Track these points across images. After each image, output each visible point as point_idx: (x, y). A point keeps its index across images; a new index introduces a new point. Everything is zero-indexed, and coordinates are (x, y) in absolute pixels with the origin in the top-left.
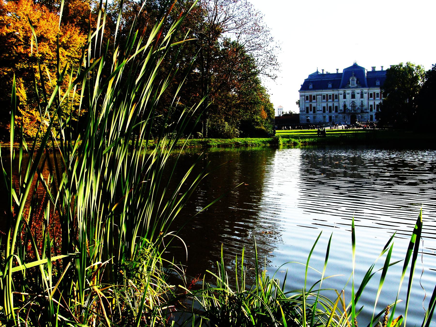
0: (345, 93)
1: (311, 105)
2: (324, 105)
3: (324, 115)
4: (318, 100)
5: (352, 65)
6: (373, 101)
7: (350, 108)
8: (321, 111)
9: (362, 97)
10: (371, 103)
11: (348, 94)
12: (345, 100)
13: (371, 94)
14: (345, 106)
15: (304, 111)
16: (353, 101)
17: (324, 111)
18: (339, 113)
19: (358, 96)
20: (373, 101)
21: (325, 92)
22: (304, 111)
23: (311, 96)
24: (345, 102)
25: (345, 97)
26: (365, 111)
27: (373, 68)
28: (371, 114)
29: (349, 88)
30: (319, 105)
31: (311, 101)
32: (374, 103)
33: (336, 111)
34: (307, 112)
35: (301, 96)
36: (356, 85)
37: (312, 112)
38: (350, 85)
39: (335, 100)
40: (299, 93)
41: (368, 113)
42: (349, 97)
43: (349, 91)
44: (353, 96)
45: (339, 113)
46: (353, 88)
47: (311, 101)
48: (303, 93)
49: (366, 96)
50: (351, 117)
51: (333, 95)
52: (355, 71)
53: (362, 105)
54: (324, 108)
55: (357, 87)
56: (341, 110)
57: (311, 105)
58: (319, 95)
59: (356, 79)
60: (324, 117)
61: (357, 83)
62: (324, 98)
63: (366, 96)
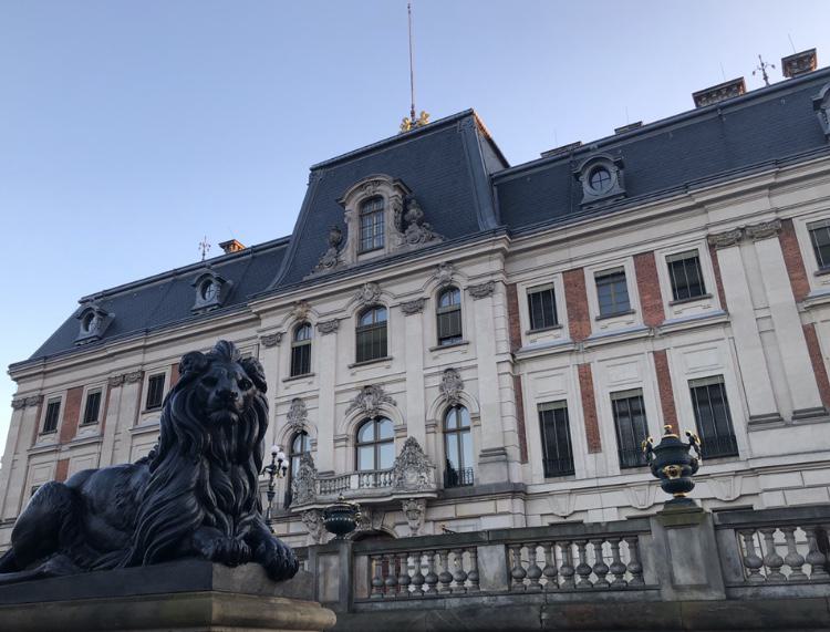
0: (302, 326)
4: (111, 421)
10: (553, 382)
11: (330, 328)
16: (368, 390)
19: (410, 336)
20: (571, 362)
23: (75, 393)
26: (489, 476)
35: (19, 404)
36: (393, 243)
38: (348, 257)
40: (13, 387)
44: (372, 347)
47: (68, 435)
48: (36, 384)
49: (485, 321)
58: (122, 380)
61: (403, 226)
63: (485, 321)
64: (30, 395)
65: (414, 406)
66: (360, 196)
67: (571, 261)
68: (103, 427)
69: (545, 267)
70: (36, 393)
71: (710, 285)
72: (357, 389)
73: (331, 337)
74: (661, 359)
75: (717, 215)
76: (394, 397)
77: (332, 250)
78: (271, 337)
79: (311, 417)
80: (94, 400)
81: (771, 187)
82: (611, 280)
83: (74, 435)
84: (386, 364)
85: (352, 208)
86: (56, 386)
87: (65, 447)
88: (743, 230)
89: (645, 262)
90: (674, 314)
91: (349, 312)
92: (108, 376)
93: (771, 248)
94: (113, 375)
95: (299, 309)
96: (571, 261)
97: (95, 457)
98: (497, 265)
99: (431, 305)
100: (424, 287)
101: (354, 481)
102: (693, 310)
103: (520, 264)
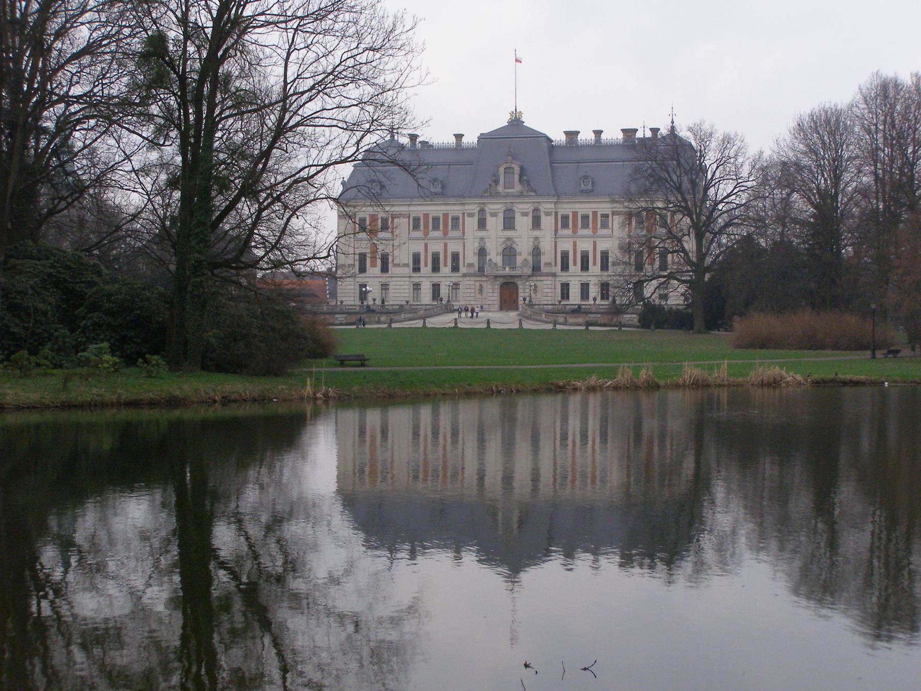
0: (482, 211)
2: (418, 247)
3: (416, 280)
5: (501, 121)
6: (571, 241)
7: (498, 260)
8: (407, 265)
9: (536, 223)
11: (494, 215)
12: (482, 234)
13: (565, 218)
14: (482, 252)
16: (509, 239)
17: (417, 269)
18: (465, 275)
19: (523, 223)
20: (571, 241)
21: (419, 209)
24: (482, 239)
25: (482, 224)
27: (572, 135)
28: (564, 280)
29: (497, 195)
32: (575, 245)
33: (455, 269)
36: (518, 188)
37: (377, 270)
38: (500, 188)
39: (452, 234)
41: (554, 275)
42: (495, 224)
43: (496, 207)
44: (509, 223)
46: (507, 196)
49: (547, 222)
50: (503, 286)
51: (446, 216)
52: (515, 139)
53: (537, 252)
54: (416, 259)
55: (521, 195)
56: (470, 265)
58: (400, 215)
59: (517, 170)
60: (417, 287)
61: (520, 181)
62: (416, 226)
65: (524, 248)
66: (505, 166)
69: (566, 209)
73: (494, 218)
74: (595, 243)
77: (493, 184)
80: (385, 221)
82: (585, 218)
85: (502, 170)
86: (365, 212)
89: (595, 214)
90: (602, 232)
91: (502, 210)
98: (553, 206)
99: (531, 214)
100: (528, 207)
101: (507, 269)
102: (605, 232)
103: (559, 206)
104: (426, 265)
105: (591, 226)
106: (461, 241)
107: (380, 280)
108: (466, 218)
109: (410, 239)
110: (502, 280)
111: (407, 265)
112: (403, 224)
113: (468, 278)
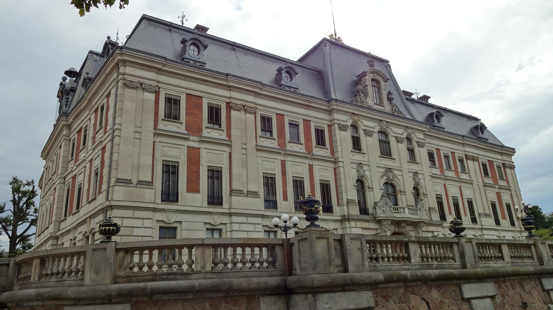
1: (194, 157)
4: (234, 132)
8: (255, 194)
11: (368, 134)
15: (150, 184)
22: (150, 184)
24: (360, 165)
25: (357, 144)
30: (245, 164)
31: (194, 129)
34: (170, 195)
37: (199, 199)
38: (370, 101)
45: (344, 219)
47: (194, 129)
51: (307, 123)
54: (269, 182)
57: (194, 157)
64: (148, 82)
67: (438, 145)
68: (229, 135)
70: (154, 84)
71: (467, 172)
72: (384, 168)
75: (467, 149)
76: (398, 176)
78: (344, 125)
79: (367, 173)
81: (476, 147)
83: (201, 130)
84: (394, 161)
87: (192, 138)
88: (473, 156)
92: (228, 100)
93: (476, 163)
94: (232, 100)
95: (356, 117)
96: (438, 145)
97: (226, 156)
104: (285, 198)
105: (453, 168)
106: (332, 165)
107: (207, 219)
108: (337, 132)
109: (260, 149)
110: (393, 229)
111: (255, 194)
112: (243, 124)
113: (353, 224)
